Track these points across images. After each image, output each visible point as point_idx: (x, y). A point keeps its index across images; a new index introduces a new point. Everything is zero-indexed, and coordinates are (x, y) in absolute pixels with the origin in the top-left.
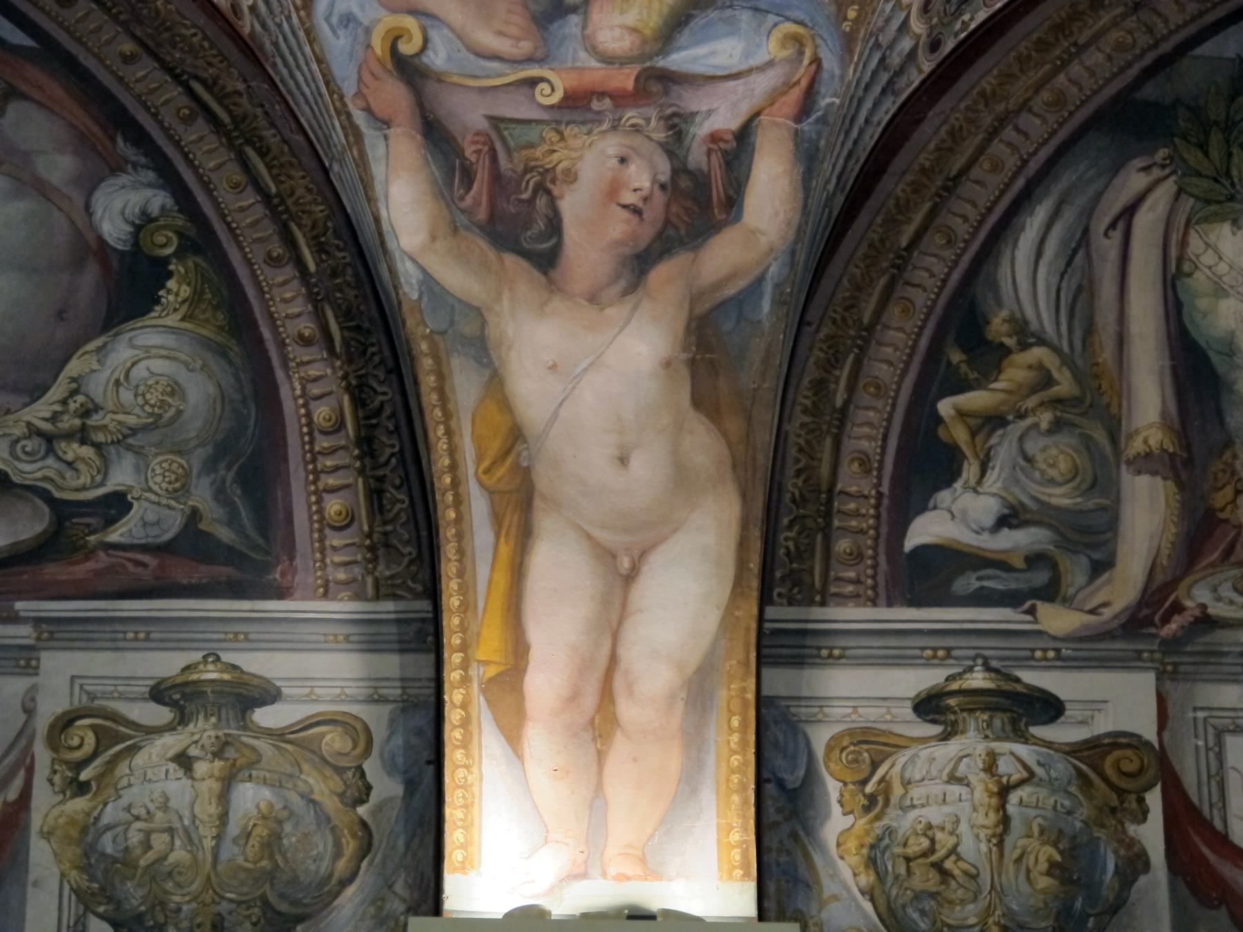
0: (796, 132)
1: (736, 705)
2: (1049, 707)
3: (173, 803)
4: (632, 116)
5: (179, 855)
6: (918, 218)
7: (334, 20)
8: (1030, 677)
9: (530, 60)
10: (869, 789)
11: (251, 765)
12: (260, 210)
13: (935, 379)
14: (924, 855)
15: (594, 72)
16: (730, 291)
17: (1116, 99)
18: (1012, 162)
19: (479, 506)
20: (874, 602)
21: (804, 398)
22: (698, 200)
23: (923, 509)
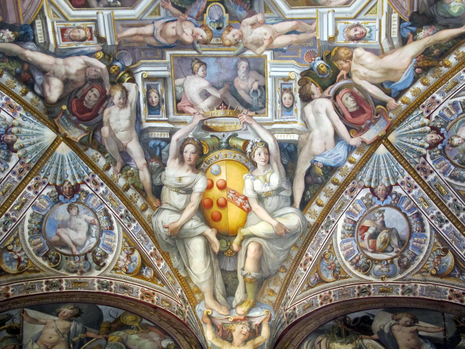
4: (243, 322)
6: (288, 344)
9: (228, 315)
12: (187, 343)
15: (237, 317)
17: (316, 329)
18: (301, 337)
22: (254, 332)
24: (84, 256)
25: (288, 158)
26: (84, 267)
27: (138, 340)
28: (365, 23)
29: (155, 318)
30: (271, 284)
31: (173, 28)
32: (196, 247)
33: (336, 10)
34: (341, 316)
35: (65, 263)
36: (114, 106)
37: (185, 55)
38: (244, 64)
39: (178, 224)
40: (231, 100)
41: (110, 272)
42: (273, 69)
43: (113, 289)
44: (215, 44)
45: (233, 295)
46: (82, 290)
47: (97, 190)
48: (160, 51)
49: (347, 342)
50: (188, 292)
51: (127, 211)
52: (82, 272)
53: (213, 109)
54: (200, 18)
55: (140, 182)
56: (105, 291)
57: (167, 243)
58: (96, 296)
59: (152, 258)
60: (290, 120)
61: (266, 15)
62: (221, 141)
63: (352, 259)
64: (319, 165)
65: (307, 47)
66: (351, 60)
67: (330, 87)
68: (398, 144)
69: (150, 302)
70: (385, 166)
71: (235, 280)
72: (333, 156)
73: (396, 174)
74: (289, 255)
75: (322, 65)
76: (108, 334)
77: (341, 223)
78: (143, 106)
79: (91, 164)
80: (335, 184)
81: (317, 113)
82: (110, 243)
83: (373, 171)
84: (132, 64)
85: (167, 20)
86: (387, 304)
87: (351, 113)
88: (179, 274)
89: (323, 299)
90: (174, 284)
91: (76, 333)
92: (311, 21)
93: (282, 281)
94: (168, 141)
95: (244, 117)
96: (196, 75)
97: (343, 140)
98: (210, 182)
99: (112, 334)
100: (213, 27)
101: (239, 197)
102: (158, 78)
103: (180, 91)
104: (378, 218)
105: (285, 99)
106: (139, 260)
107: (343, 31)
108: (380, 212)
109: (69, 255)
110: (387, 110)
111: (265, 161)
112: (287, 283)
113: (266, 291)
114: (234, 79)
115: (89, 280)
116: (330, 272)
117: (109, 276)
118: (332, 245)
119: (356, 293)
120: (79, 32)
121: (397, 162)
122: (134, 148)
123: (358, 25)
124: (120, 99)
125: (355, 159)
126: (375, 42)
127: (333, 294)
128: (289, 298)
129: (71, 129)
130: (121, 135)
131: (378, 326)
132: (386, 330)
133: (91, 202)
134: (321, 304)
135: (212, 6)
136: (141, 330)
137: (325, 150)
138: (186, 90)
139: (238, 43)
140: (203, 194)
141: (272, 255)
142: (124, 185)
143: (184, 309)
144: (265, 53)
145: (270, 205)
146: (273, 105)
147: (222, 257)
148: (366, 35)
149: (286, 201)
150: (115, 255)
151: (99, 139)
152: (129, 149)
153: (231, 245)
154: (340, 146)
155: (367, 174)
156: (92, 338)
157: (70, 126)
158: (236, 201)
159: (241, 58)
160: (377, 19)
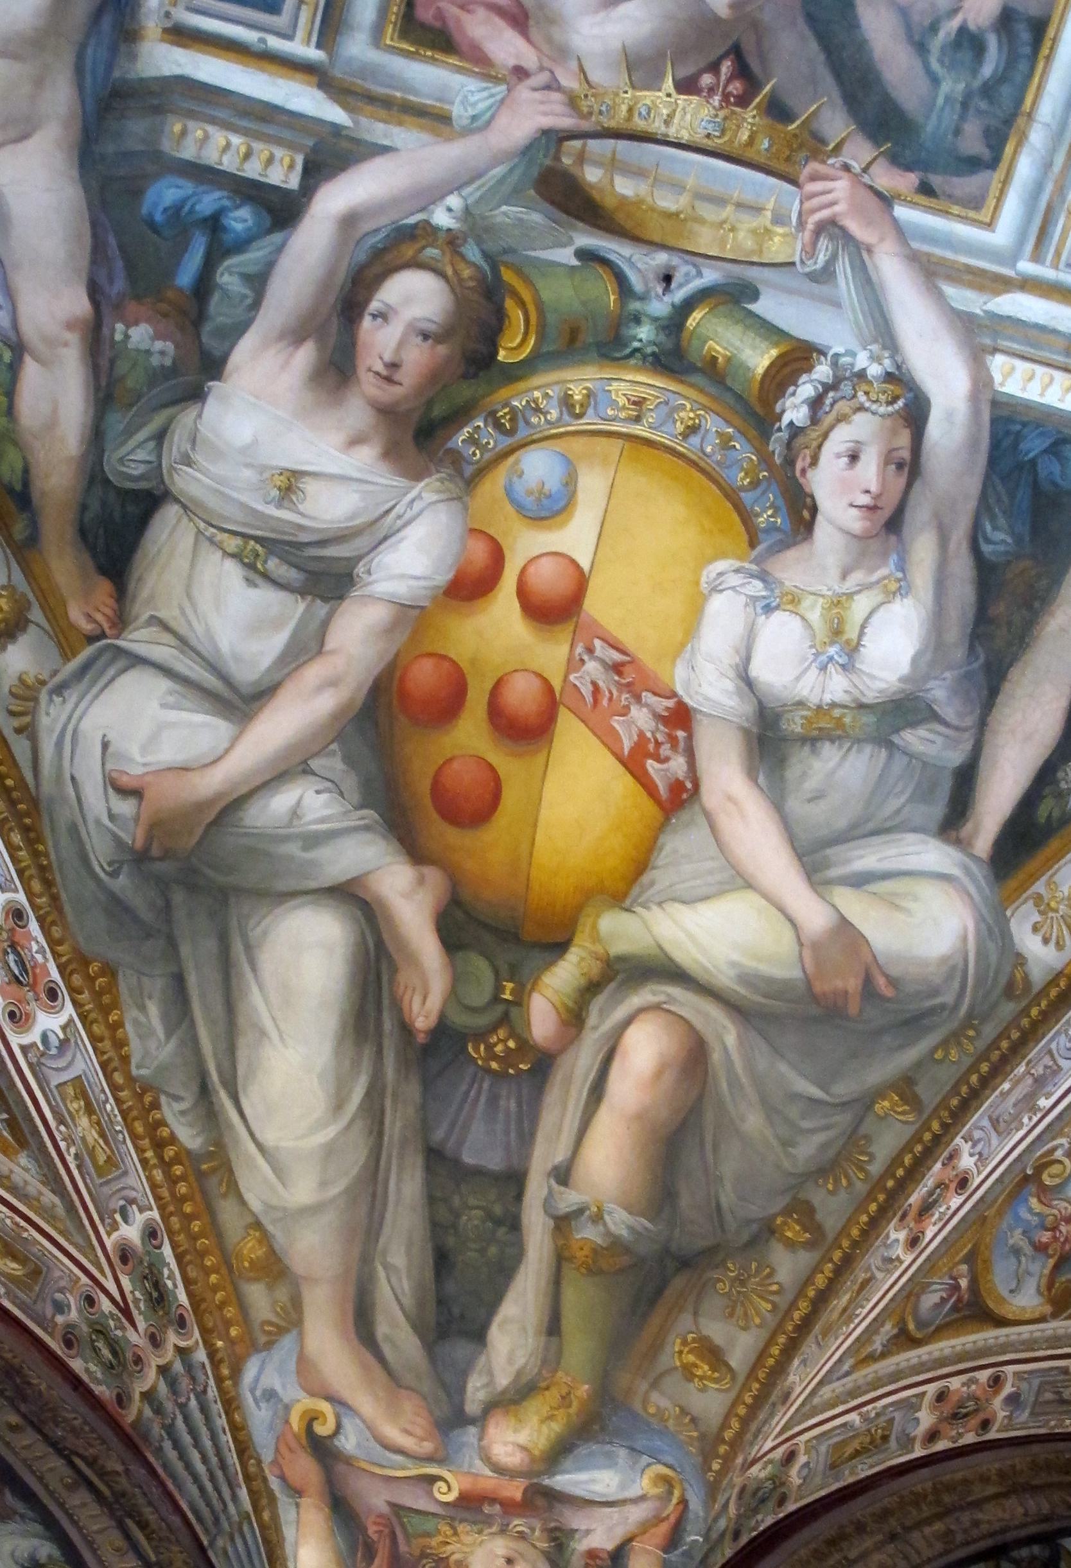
4: (518, 1524)
7: (258, 1393)
9: (430, 1459)
15: (488, 1480)
25: (1024, 529)
30: (713, 1303)
32: (302, 960)
34: (1031, 1540)
45: (479, 1336)
50: (202, 1254)
53: (653, 82)
62: (635, 306)
71: (501, 1232)
74: (854, 1142)
88: (162, 1123)
89: (947, 1409)
93: (783, 1302)
94: (282, 211)
95: (841, 187)
98: (479, 552)
101: (638, 698)
111: (872, 509)
116: (1035, 1267)
127: (1008, 1389)
134: (932, 1436)
140: (414, 620)
141: (753, 1121)
146: (1048, 165)
147: (450, 1068)
149: (924, 794)
153: (520, 1001)
158: (617, 723)
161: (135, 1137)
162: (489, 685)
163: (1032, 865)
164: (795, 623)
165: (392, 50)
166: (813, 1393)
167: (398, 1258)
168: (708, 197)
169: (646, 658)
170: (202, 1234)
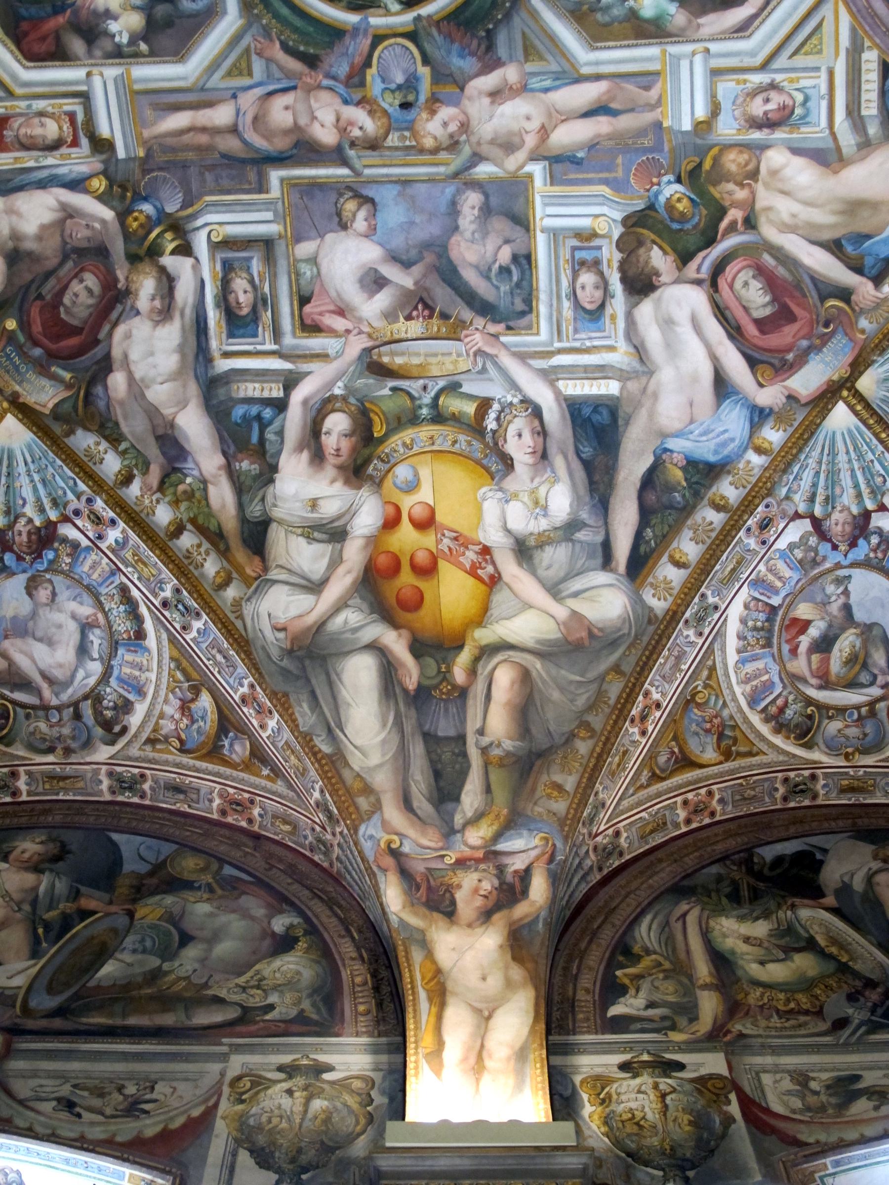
0: (548, 870)
1: (538, 1059)
2: (681, 1067)
3: (283, 1107)
4: (482, 866)
5: (284, 1125)
6: (599, 921)
8: (668, 1056)
9: (442, 849)
10: (602, 1096)
11: (319, 1093)
13: (611, 965)
14: (630, 1119)
15: (467, 852)
16: (526, 921)
18: (634, 903)
19: (422, 995)
20: (596, 1033)
21: (559, 971)
22: (511, 891)
23: (613, 1004)
24: (71, 709)
25: (595, 444)
26: (73, 738)
27: (211, 915)
28: (791, 81)
29: (257, 863)
30: (555, 768)
31: (287, 108)
32: (359, 676)
33: (714, 47)
35: (25, 727)
36: (138, 317)
37: (320, 178)
38: (472, 200)
39: (311, 619)
40: (441, 294)
41: (140, 749)
42: (551, 210)
43: (149, 792)
44: (397, 148)
45: (457, 799)
46: (68, 798)
47: (100, 537)
48: (255, 169)
49: (755, 915)
50: (337, 791)
51: (178, 591)
52: (68, 751)
53: (396, 320)
54: (356, 79)
55: (210, 514)
56: (129, 797)
57: (282, 668)
58: (104, 811)
59: (245, 710)
60: (596, 343)
61: (530, 67)
62: (418, 402)
63: (766, 707)
64: (675, 461)
65: (637, 149)
66: (756, 181)
67: (701, 254)
68: (883, 401)
69: (244, 824)
70: (850, 461)
71: (460, 759)
72: (711, 436)
73: (879, 480)
74: (600, 694)
75: (677, 196)
76: (134, 901)
77: (736, 611)
78: (213, 316)
79: (84, 468)
80: (718, 508)
81: (667, 323)
82: (137, 673)
83: (817, 474)
84: (183, 207)
85: (271, 88)
86: (859, 822)
87: (759, 323)
88: (315, 746)
89: (691, 808)
90: (304, 773)
91: (52, 899)
92: (646, 79)
93: (584, 762)
94: (280, 406)
95: (478, 336)
96: (350, 231)
97: (737, 393)
98: (391, 510)
99: (142, 903)
100: (390, 103)
101: (467, 548)
102: (250, 241)
103: (308, 273)
104: (833, 598)
105: (583, 288)
106: (212, 716)
107: (734, 103)
108: (839, 581)
109: (33, 707)
110: (853, 310)
111: (534, 452)
112: (595, 766)
113: (541, 788)
114: (449, 238)
115: (86, 771)
116: (709, 740)
117: (136, 759)
118: (713, 669)
119: (778, 795)
120: (43, 125)
121: (880, 448)
122: (194, 426)
123: (773, 86)
124: (153, 299)
125: (771, 443)
126: (817, 129)
127: (717, 797)
128: (603, 805)
129: (29, 381)
130: (159, 394)
131: (837, 876)
132: (858, 884)
133: (86, 568)
134: (688, 821)
135: (386, 48)
136: (220, 892)
137: (692, 422)
138: (324, 271)
139: (457, 143)
140: (373, 541)
141: (556, 695)
142: (170, 523)
143: (329, 837)
144: (528, 168)
145: (548, 568)
146: (551, 306)
147: (427, 702)
148: (792, 112)
149: (591, 556)
150: (152, 704)
151: (101, 404)
152: (180, 428)
153: (449, 670)
154: (731, 411)
155: (802, 483)
156: (94, 913)
157: (27, 371)
158: (461, 559)
159: (465, 184)
160: (824, 69)
161: (307, 754)
162: (408, 558)
163: (645, 571)
164: (519, 504)
165: (300, 337)
166: (618, 804)
167: (418, 777)
168: (430, 355)
169: (466, 531)
170: (337, 783)
